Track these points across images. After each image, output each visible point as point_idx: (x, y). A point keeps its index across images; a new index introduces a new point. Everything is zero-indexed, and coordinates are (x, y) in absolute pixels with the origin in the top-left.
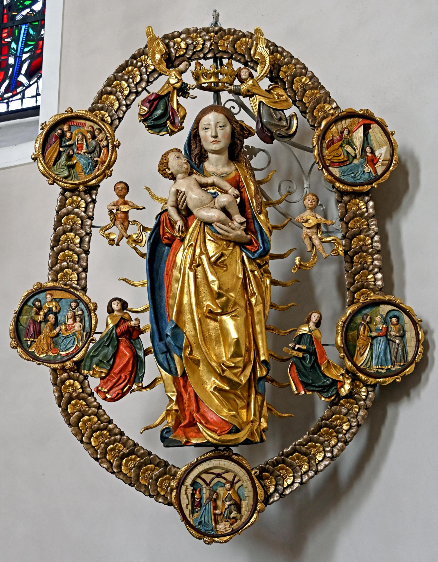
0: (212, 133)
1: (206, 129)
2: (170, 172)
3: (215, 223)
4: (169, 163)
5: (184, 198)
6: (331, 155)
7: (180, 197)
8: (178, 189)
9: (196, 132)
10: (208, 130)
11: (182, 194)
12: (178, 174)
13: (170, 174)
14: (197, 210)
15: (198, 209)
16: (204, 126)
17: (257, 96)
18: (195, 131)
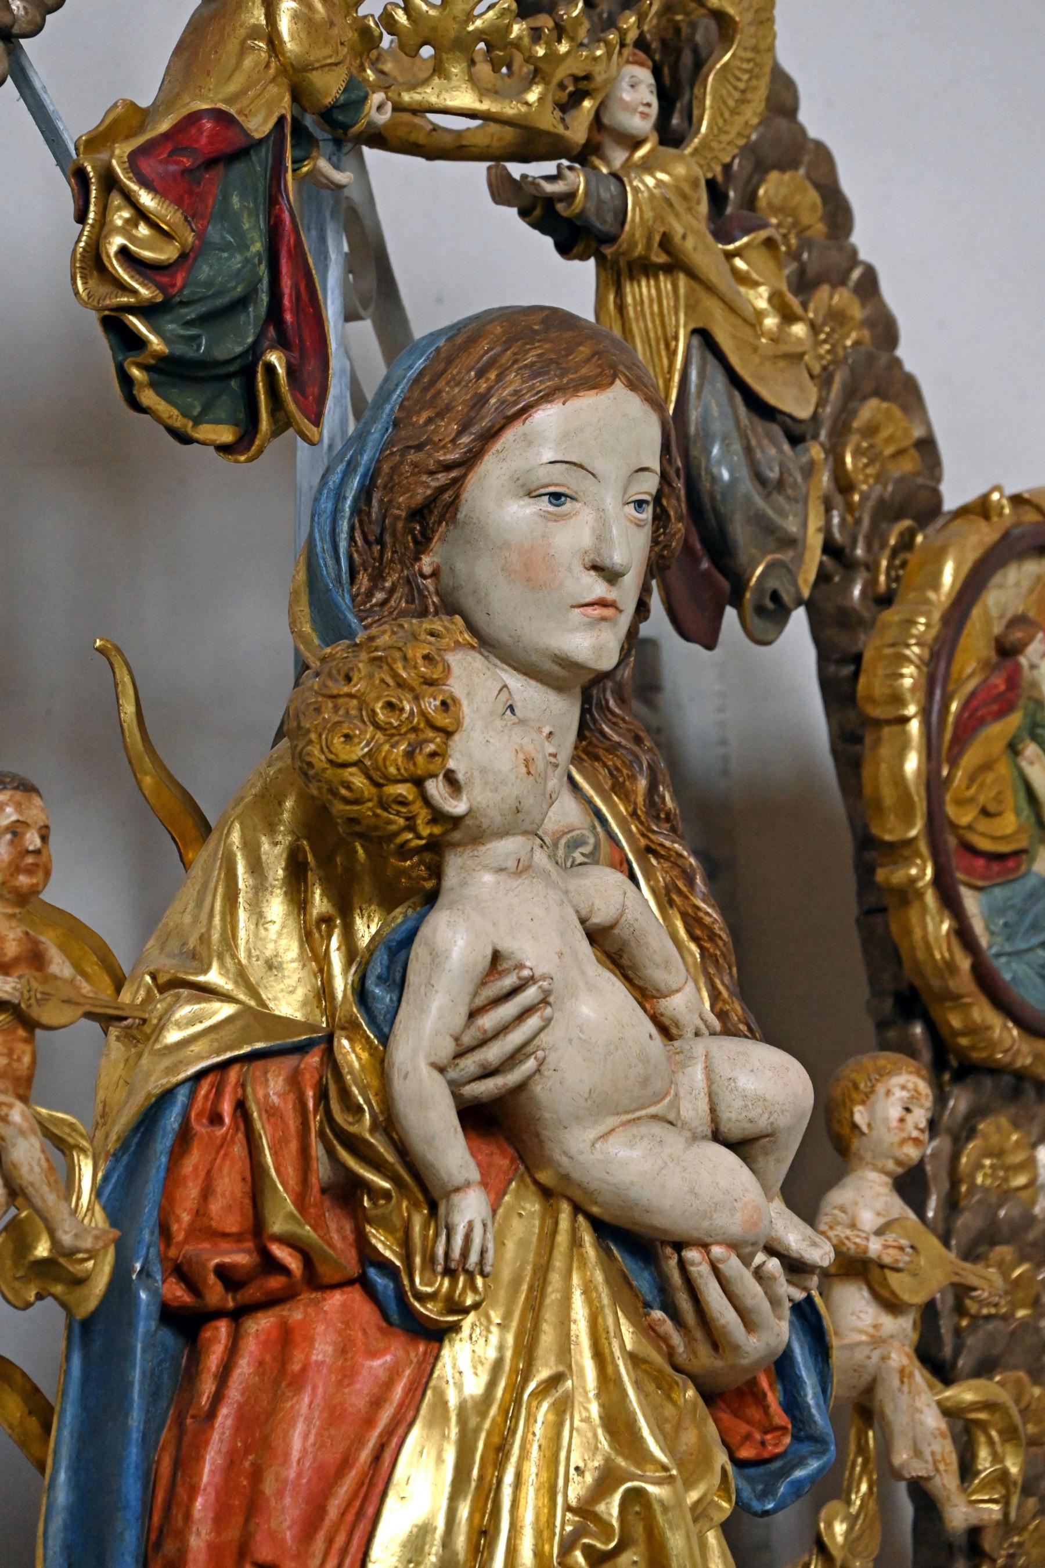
0: (602, 537)
1: (556, 497)
2: (458, 807)
3: (717, 1251)
4: (456, 737)
5: (533, 1022)
6: (971, 800)
7: (508, 1010)
8: (506, 945)
9: (441, 490)
10: (568, 506)
11: (531, 994)
12: (503, 833)
13: (438, 816)
14: (602, 1129)
15: (611, 1121)
16: (544, 475)
17: (682, 280)
18: (443, 478)
